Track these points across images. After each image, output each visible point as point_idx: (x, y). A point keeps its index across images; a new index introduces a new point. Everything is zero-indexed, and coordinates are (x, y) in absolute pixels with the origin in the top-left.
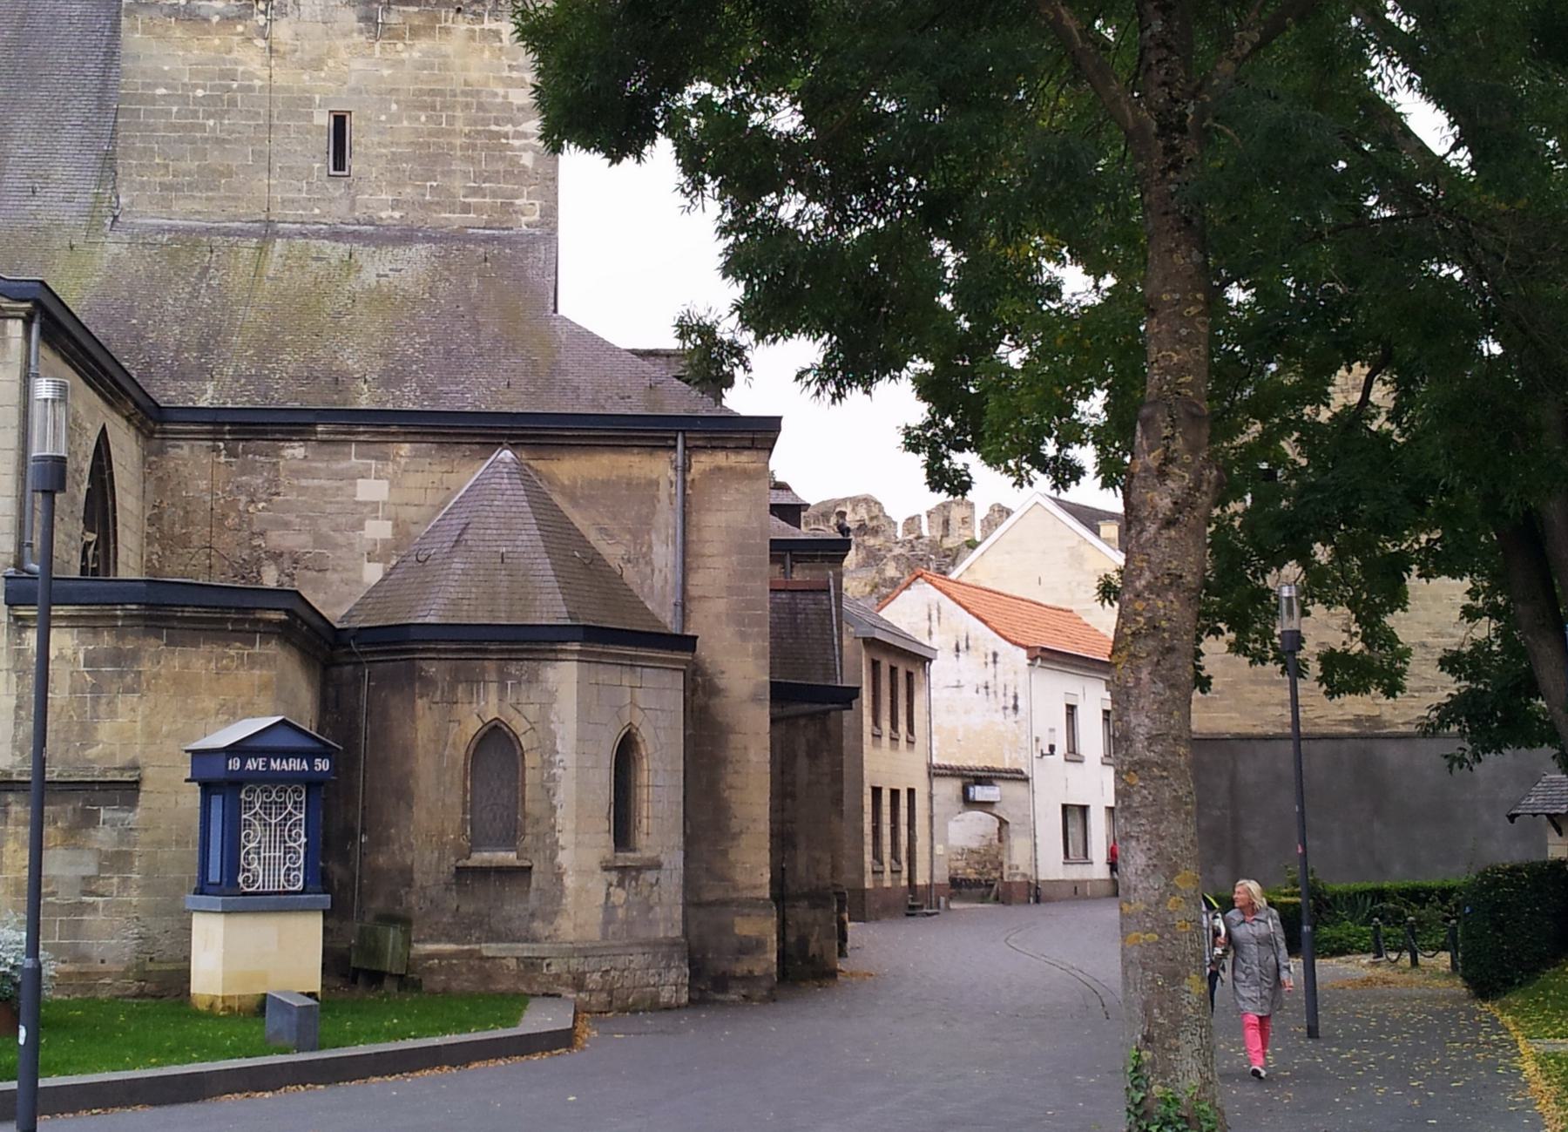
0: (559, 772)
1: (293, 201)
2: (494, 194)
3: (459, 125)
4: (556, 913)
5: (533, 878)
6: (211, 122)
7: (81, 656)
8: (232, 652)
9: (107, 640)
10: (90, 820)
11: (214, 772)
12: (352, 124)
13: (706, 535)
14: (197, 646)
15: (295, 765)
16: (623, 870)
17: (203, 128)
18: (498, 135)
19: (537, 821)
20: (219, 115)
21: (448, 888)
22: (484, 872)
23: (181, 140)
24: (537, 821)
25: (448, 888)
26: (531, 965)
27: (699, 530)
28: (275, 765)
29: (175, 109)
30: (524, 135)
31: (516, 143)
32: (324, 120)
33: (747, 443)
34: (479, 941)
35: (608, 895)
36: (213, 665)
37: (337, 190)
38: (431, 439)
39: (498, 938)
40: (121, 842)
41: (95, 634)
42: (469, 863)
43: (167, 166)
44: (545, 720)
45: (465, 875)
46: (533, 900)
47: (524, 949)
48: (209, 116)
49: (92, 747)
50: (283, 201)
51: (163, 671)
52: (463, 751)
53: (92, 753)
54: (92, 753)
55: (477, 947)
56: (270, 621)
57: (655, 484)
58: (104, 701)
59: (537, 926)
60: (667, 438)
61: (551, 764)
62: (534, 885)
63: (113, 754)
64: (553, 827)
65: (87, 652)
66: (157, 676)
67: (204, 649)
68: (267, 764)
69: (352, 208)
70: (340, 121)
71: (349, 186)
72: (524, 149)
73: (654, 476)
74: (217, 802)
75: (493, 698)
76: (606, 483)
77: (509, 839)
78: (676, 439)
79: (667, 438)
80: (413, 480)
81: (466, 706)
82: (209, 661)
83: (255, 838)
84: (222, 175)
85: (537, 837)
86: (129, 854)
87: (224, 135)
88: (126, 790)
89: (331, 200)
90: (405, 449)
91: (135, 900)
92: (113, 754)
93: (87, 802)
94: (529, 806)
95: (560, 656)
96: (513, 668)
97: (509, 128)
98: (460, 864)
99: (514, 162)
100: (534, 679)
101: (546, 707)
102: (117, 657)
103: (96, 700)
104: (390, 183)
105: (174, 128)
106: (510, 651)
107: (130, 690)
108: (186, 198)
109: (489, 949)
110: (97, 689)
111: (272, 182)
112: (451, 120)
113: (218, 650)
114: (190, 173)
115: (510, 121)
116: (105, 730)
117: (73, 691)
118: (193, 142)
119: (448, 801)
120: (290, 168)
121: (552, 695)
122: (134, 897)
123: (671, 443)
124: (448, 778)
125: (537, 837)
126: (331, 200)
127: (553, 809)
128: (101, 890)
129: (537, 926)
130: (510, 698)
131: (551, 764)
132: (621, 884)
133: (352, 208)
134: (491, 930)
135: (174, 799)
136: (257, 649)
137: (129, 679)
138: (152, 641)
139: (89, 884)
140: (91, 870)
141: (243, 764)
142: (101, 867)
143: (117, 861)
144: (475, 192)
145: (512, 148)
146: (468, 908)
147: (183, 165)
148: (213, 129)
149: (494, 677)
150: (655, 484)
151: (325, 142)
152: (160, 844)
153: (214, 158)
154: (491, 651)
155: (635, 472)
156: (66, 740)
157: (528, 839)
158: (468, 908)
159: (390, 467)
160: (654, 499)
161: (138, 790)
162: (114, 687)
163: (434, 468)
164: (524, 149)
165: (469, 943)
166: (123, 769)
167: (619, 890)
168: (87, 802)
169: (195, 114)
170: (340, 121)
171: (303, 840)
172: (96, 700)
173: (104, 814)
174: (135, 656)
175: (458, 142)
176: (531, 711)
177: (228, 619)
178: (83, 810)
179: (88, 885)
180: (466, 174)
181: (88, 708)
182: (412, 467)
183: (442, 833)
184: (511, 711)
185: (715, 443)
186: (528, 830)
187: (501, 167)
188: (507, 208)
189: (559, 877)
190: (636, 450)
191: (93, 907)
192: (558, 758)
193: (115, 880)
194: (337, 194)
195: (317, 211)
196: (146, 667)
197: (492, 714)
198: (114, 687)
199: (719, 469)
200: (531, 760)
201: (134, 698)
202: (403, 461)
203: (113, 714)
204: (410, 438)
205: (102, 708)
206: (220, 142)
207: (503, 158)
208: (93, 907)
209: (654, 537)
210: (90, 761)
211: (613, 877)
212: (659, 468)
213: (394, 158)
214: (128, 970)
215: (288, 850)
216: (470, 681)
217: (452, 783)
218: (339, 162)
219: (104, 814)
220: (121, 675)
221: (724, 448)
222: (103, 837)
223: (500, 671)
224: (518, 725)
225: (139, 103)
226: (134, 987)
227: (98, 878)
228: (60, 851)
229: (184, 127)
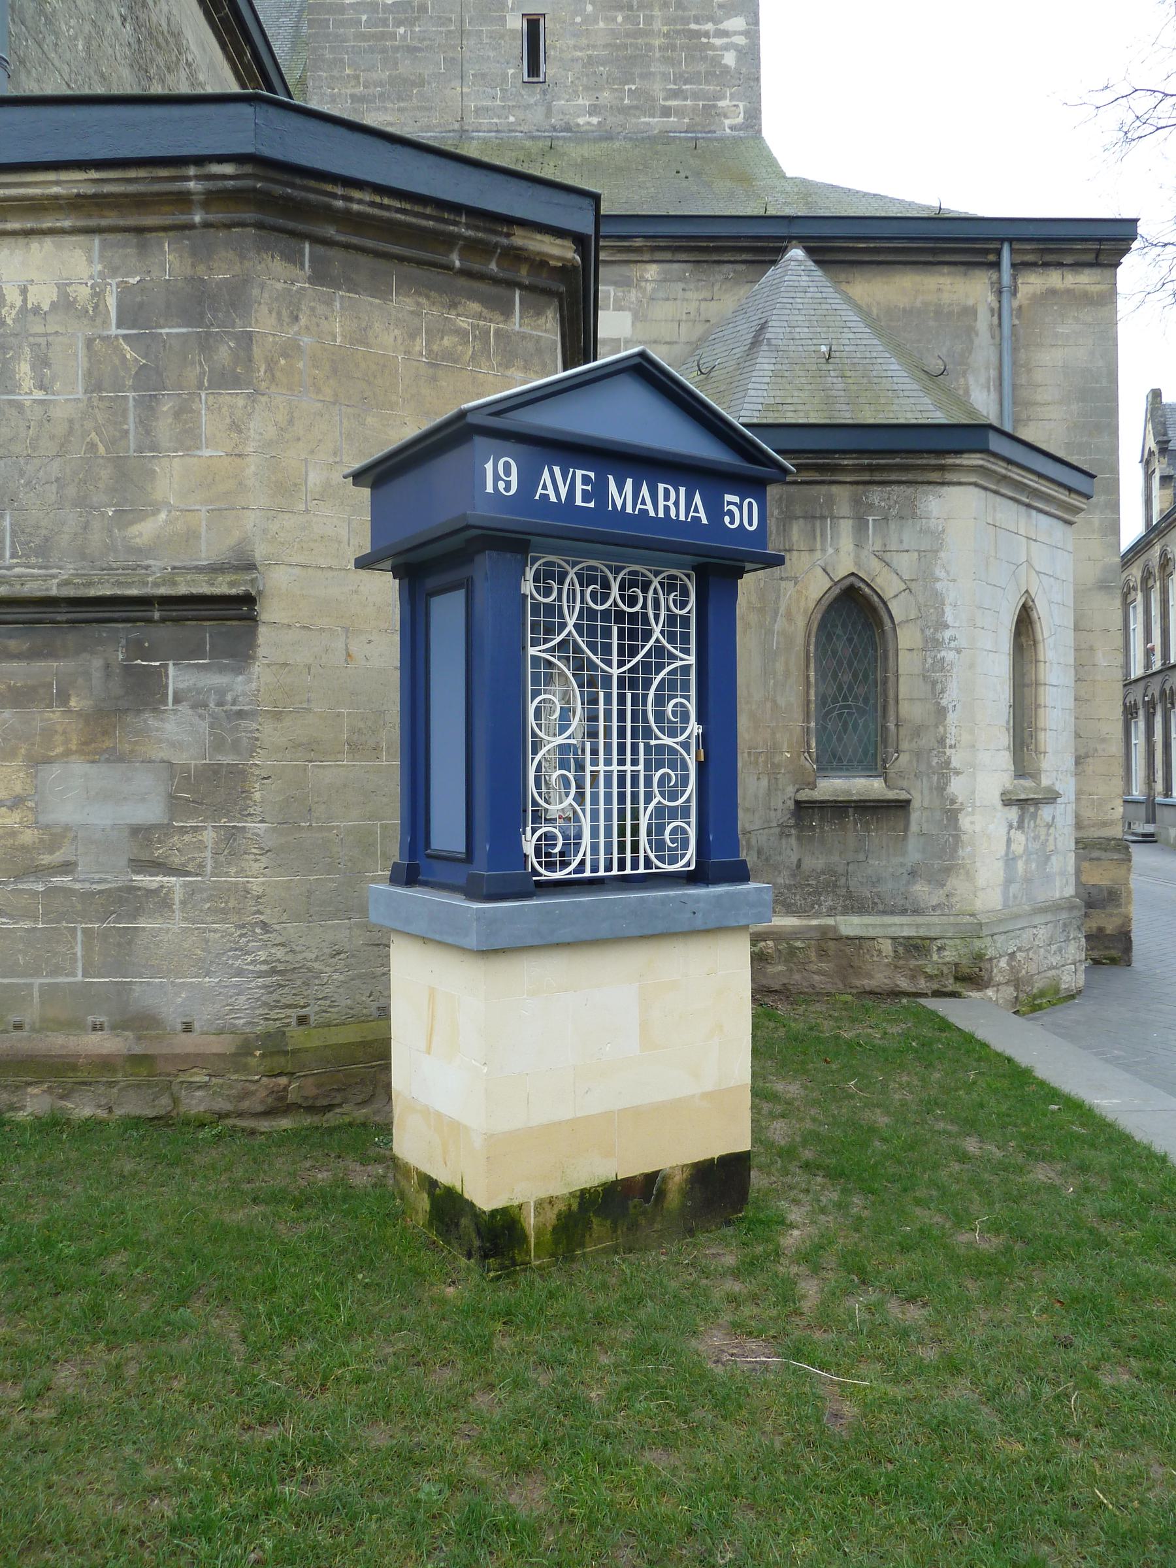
0: (950, 656)
1: (487, 109)
2: (695, 96)
3: (657, 25)
4: (948, 870)
5: (915, 816)
6: (402, 30)
7: (111, 302)
8: (463, 323)
9: (169, 262)
10: (143, 690)
11: (438, 503)
12: (547, 27)
13: (1039, 376)
14: (385, 295)
15: (672, 503)
16: (1022, 803)
17: (393, 36)
18: (698, 34)
19: (918, 731)
20: (410, 22)
21: (783, 834)
22: (838, 809)
23: (372, 50)
24: (918, 731)
25: (783, 834)
26: (915, 947)
27: (1029, 371)
28: (622, 495)
29: (364, 18)
30: (725, 34)
31: (718, 42)
32: (517, 24)
33: (1090, 257)
34: (832, 912)
35: (1009, 841)
36: (420, 344)
37: (532, 97)
38: (684, 257)
39: (857, 906)
40: (218, 744)
41: (143, 248)
42: (816, 795)
43: (357, 77)
44: (927, 576)
45: (806, 811)
46: (913, 853)
47: (904, 926)
48: (399, 24)
49: (141, 516)
50: (477, 110)
51: (306, 340)
52: (801, 622)
53: (144, 531)
54: (144, 531)
55: (830, 921)
56: (540, 264)
57: (970, 312)
58: (166, 407)
59: (921, 890)
60: (987, 251)
61: (937, 644)
62: (914, 828)
63: (191, 536)
64: (942, 741)
65: (125, 291)
66: (290, 350)
67: (403, 304)
68: (598, 492)
69: (549, 113)
70: (533, 25)
71: (544, 92)
72: (726, 48)
73: (970, 302)
74: (447, 613)
75: (846, 542)
76: (908, 312)
77: (873, 760)
78: (998, 252)
79: (987, 251)
80: (662, 310)
81: (805, 556)
82: (413, 336)
83: (555, 718)
84: (413, 84)
85: (918, 754)
86: (238, 774)
87: (416, 43)
88: (223, 615)
89: (527, 107)
90: (652, 271)
91: (256, 884)
92: (191, 536)
93: (137, 649)
94: (905, 708)
95: (949, 477)
96: (876, 496)
97: (709, 26)
98: (804, 795)
99: (716, 61)
100: (910, 513)
101: (928, 555)
102: (199, 304)
103: (148, 406)
104: (587, 88)
105: (363, 37)
106: (871, 468)
107: (225, 380)
108: (378, 109)
109: (851, 925)
110: (150, 381)
111: (465, 90)
112: (649, 20)
113: (432, 311)
114: (381, 84)
115: (711, 19)
116: (171, 478)
117: (95, 385)
118: (384, 51)
119: (781, 702)
120: (483, 76)
121: (938, 537)
122: (256, 876)
123: (992, 258)
124: (780, 666)
125: (918, 754)
126: (527, 107)
127: (941, 712)
128: (176, 860)
129: (921, 890)
130: (874, 541)
131: (937, 644)
132: (1020, 826)
133: (549, 113)
134: (849, 895)
135: (337, 620)
136: (516, 323)
137: (224, 353)
138: (278, 265)
139: (148, 843)
140: (151, 812)
141: (529, 480)
142: (174, 804)
143: (212, 789)
144: (675, 94)
145: (713, 47)
146: (815, 862)
147: (375, 76)
148: (404, 37)
149: (843, 507)
150: (970, 312)
151: (520, 47)
152: (311, 748)
153: (406, 67)
154: (843, 469)
155: (946, 298)
156: (81, 502)
157: (904, 758)
158: (815, 862)
159: (634, 295)
160: (971, 331)
161: (253, 619)
162: (192, 374)
163: (689, 295)
164: (726, 48)
165: (818, 914)
166: (215, 569)
167: (1019, 833)
168: (137, 649)
169: (385, 22)
170: (533, 25)
171: (694, 728)
172: (148, 406)
173: (176, 677)
174: (237, 298)
175: (657, 42)
176: (905, 563)
177: (450, 241)
178: (128, 670)
179: (145, 848)
180: (665, 77)
181: (131, 425)
182: (661, 294)
183: (774, 749)
184: (875, 564)
185: (1049, 258)
186: (904, 745)
187: (702, 67)
188: (710, 112)
189: (951, 815)
190: (946, 269)
191: (161, 901)
192: (947, 634)
193: (209, 836)
194: (532, 101)
195: (512, 119)
196: (264, 323)
197: (844, 567)
198: (192, 374)
199: (1053, 292)
200: (907, 638)
201: (235, 400)
202: (649, 287)
203: (189, 439)
204: (659, 256)
205: (164, 428)
206: (412, 50)
207: (704, 59)
208: (161, 901)
209: (971, 380)
210: (139, 551)
211: (1013, 813)
212: (971, 290)
213: (591, 61)
214: (245, 1050)
215: (659, 757)
216: (810, 517)
217: (787, 674)
218: (534, 69)
219: (176, 677)
220: (206, 344)
221: (1060, 265)
222: (175, 733)
223: (856, 502)
224: (887, 584)
225: (329, 13)
226: (262, 1089)
227: (166, 829)
228: (79, 767)
229: (373, 36)
